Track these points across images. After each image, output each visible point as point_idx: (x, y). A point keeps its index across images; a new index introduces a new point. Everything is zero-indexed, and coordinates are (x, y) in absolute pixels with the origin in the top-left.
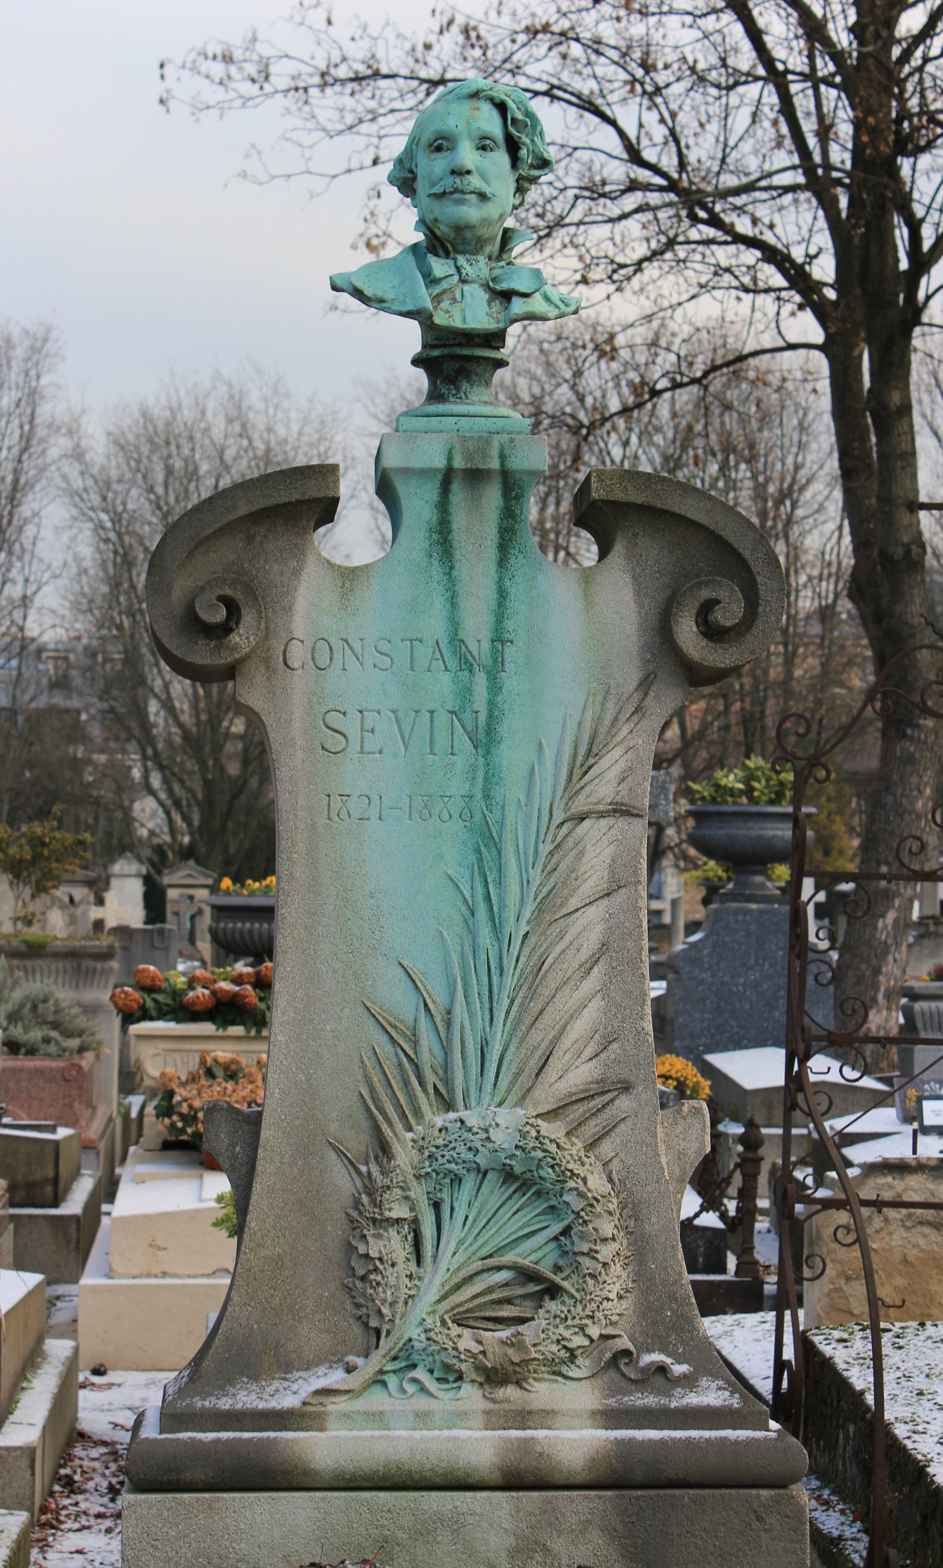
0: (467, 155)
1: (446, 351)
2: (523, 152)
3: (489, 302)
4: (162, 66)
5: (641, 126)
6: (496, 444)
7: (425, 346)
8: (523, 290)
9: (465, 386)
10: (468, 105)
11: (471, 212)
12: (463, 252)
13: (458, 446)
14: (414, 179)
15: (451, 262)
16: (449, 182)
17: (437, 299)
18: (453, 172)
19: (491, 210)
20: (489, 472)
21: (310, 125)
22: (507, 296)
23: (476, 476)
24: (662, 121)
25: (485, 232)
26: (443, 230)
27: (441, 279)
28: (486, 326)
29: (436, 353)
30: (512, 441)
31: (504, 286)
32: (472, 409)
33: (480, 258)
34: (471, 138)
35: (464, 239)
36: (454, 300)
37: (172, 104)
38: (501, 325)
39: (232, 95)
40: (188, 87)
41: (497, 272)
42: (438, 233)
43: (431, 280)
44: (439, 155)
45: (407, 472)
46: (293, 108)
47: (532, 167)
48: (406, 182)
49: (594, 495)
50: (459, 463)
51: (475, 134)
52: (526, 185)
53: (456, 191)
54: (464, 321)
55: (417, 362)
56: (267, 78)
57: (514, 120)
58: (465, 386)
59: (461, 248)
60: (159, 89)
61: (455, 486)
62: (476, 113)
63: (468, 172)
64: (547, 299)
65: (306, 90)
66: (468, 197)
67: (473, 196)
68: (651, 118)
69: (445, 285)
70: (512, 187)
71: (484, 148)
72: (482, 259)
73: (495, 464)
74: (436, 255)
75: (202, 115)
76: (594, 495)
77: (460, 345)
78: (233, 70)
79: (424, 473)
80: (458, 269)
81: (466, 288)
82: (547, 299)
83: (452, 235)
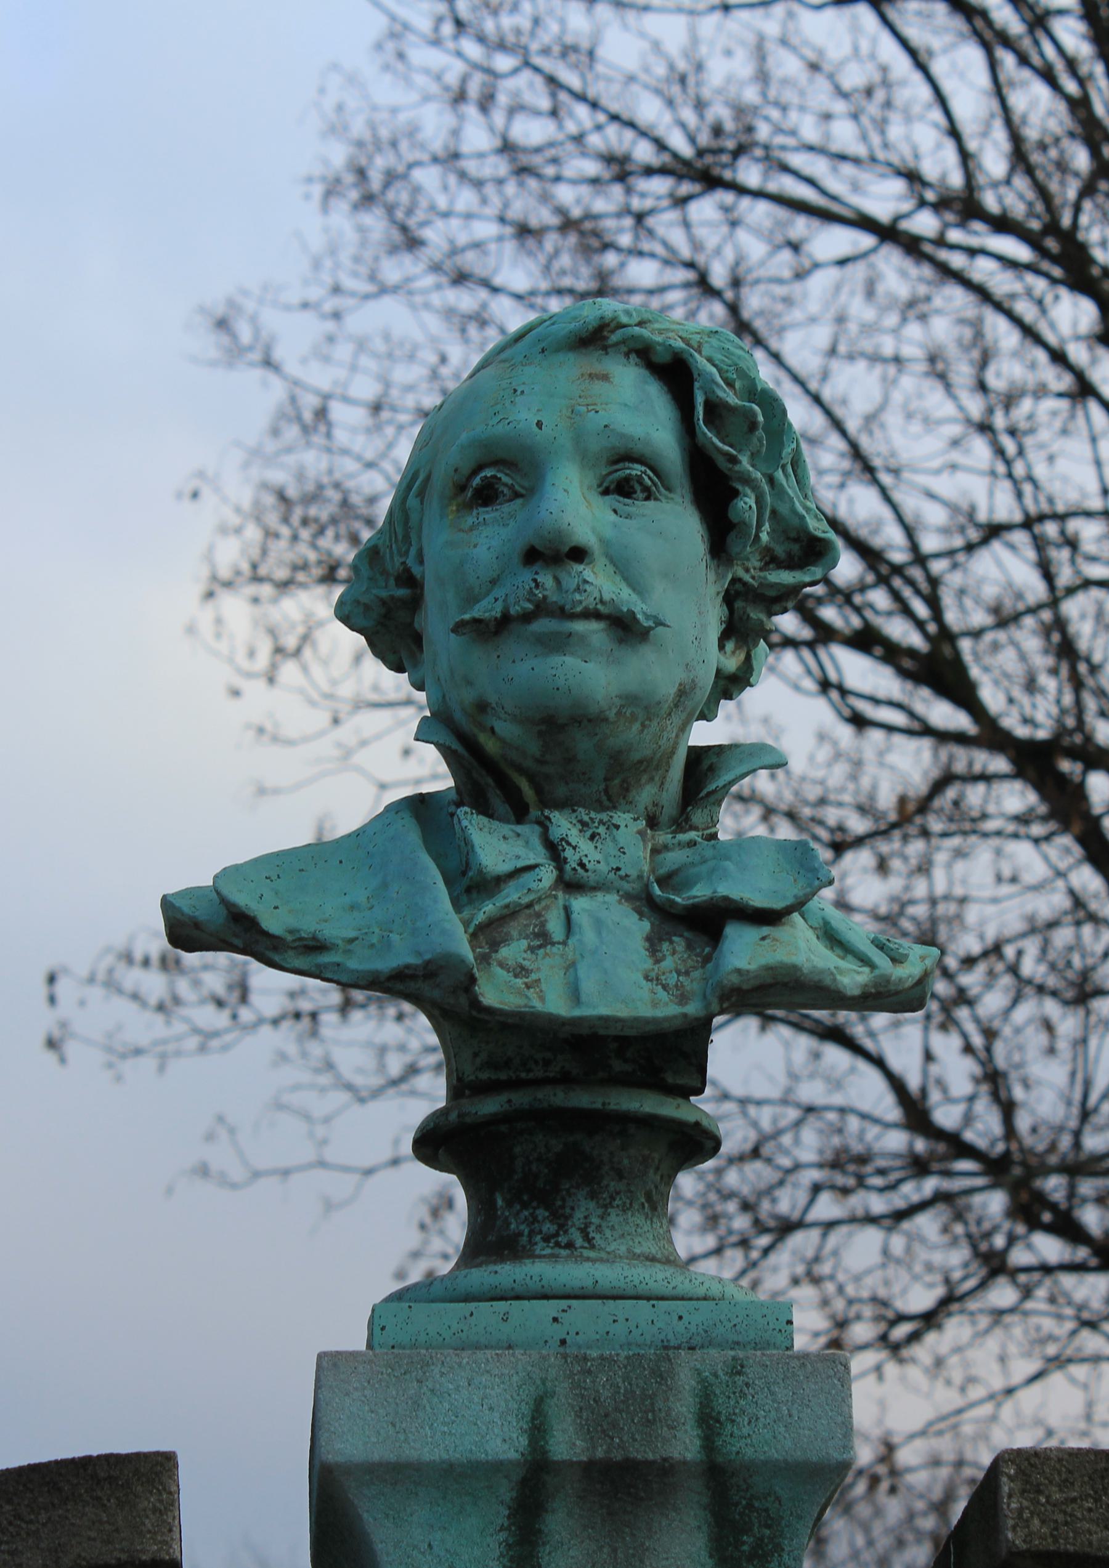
0: (573, 504)
1: (521, 1099)
2: (746, 504)
3: (653, 943)
4: (52, 979)
5: (929, 1057)
6: (686, 1380)
7: (458, 1089)
8: (758, 900)
9: (583, 1209)
10: (569, 370)
11: (592, 674)
12: (566, 804)
13: (563, 1388)
14: (415, 603)
15: (530, 831)
16: (520, 587)
17: (489, 935)
18: (532, 556)
19: (656, 671)
20: (666, 1469)
21: (325, 1079)
22: (708, 922)
23: (623, 1486)
24: (968, 1049)
25: (633, 737)
26: (505, 733)
27: (501, 880)
28: (645, 1011)
29: (490, 1106)
30: (737, 1369)
31: (700, 892)
32: (607, 1275)
33: (621, 818)
34: (584, 457)
35: (570, 760)
36: (543, 938)
37: (71, 1048)
38: (693, 1009)
39: (179, 1027)
40: (97, 1015)
41: (674, 858)
42: (490, 746)
43: (470, 884)
44: (487, 514)
45: (400, 1475)
46: (292, 1049)
47: (772, 560)
48: (389, 619)
49: (1013, 1537)
50: (566, 1443)
51: (595, 445)
52: (756, 614)
53: (541, 609)
54: (575, 995)
55: (434, 1143)
56: (244, 998)
57: (715, 410)
58: (583, 1209)
59: (561, 791)
60: (45, 1021)
61: (559, 1522)
62: (598, 387)
63: (579, 554)
64: (832, 938)
65: (314, 1016)
66: (580, 626)
67: (594, 626)
68: (946, 1045)
69: (512, 894)
70: (714, 618)
71: (623, 489)
72: (628, 825)
73: (685, 1445)
74: (483, 808)
75: (127, 1066)
76: (1013, 1537)
77: (566, 1080)
78: (183, 986)
79: (455, 1479)
80: (554, 850)
81: (580, 904)
82: (832, 938)
83: (534, 748)
